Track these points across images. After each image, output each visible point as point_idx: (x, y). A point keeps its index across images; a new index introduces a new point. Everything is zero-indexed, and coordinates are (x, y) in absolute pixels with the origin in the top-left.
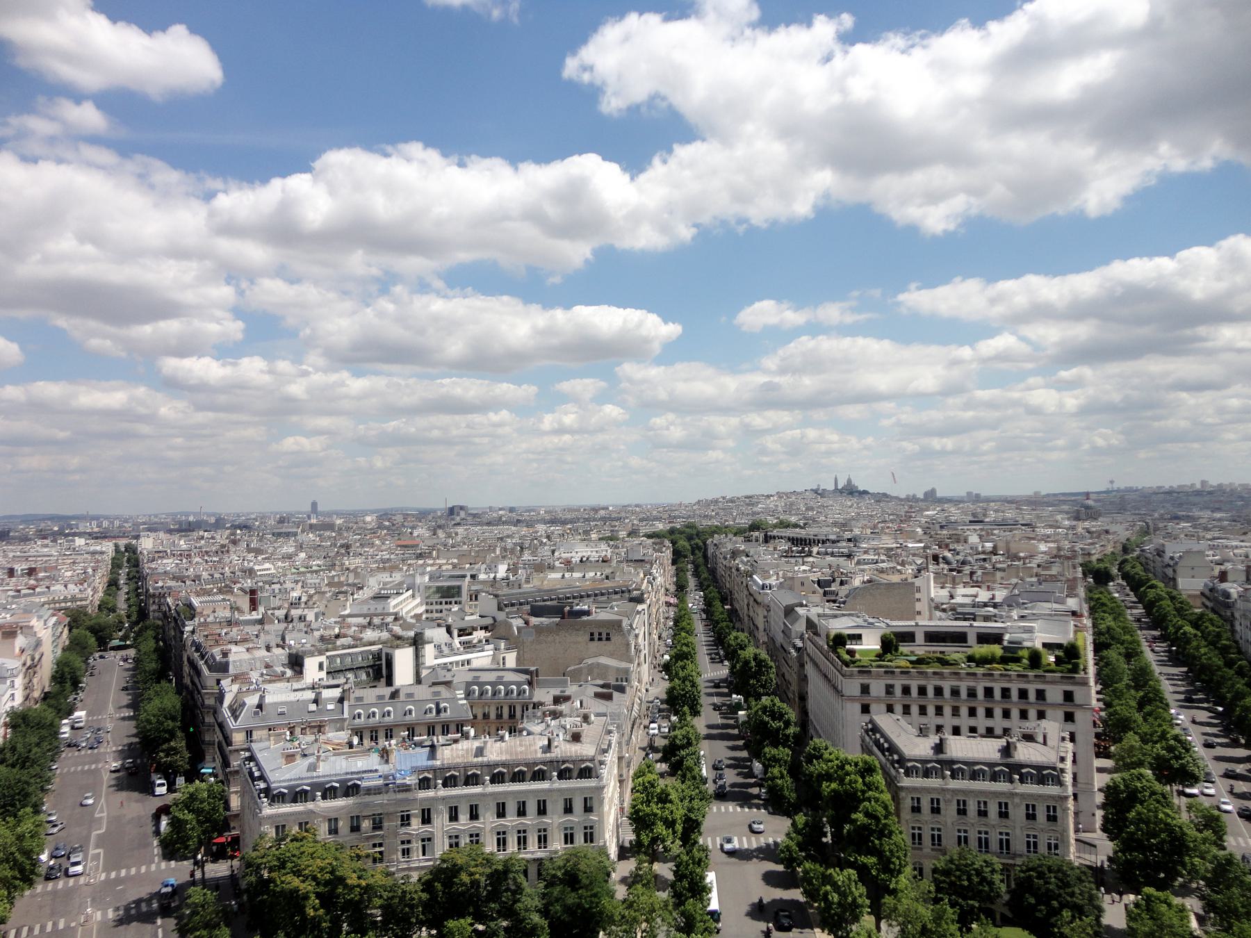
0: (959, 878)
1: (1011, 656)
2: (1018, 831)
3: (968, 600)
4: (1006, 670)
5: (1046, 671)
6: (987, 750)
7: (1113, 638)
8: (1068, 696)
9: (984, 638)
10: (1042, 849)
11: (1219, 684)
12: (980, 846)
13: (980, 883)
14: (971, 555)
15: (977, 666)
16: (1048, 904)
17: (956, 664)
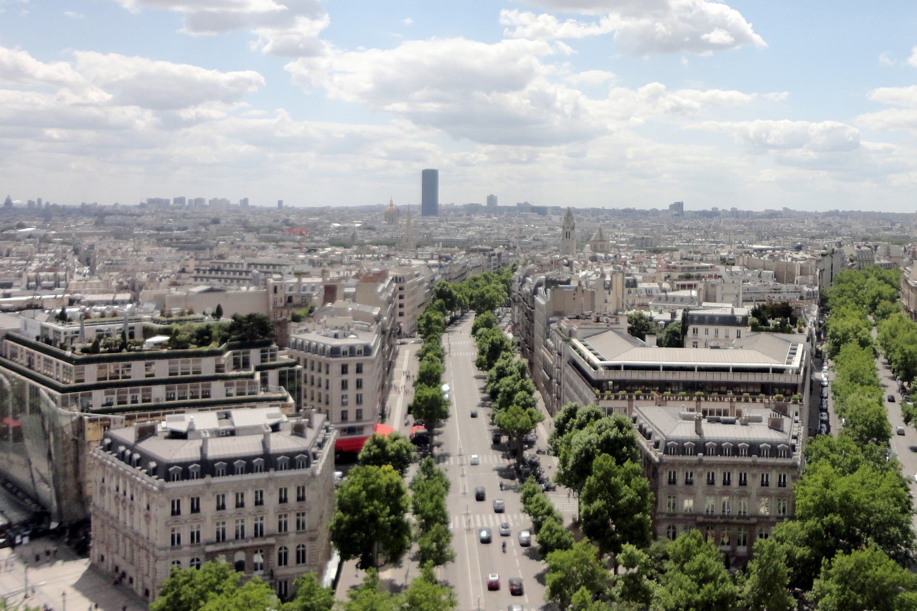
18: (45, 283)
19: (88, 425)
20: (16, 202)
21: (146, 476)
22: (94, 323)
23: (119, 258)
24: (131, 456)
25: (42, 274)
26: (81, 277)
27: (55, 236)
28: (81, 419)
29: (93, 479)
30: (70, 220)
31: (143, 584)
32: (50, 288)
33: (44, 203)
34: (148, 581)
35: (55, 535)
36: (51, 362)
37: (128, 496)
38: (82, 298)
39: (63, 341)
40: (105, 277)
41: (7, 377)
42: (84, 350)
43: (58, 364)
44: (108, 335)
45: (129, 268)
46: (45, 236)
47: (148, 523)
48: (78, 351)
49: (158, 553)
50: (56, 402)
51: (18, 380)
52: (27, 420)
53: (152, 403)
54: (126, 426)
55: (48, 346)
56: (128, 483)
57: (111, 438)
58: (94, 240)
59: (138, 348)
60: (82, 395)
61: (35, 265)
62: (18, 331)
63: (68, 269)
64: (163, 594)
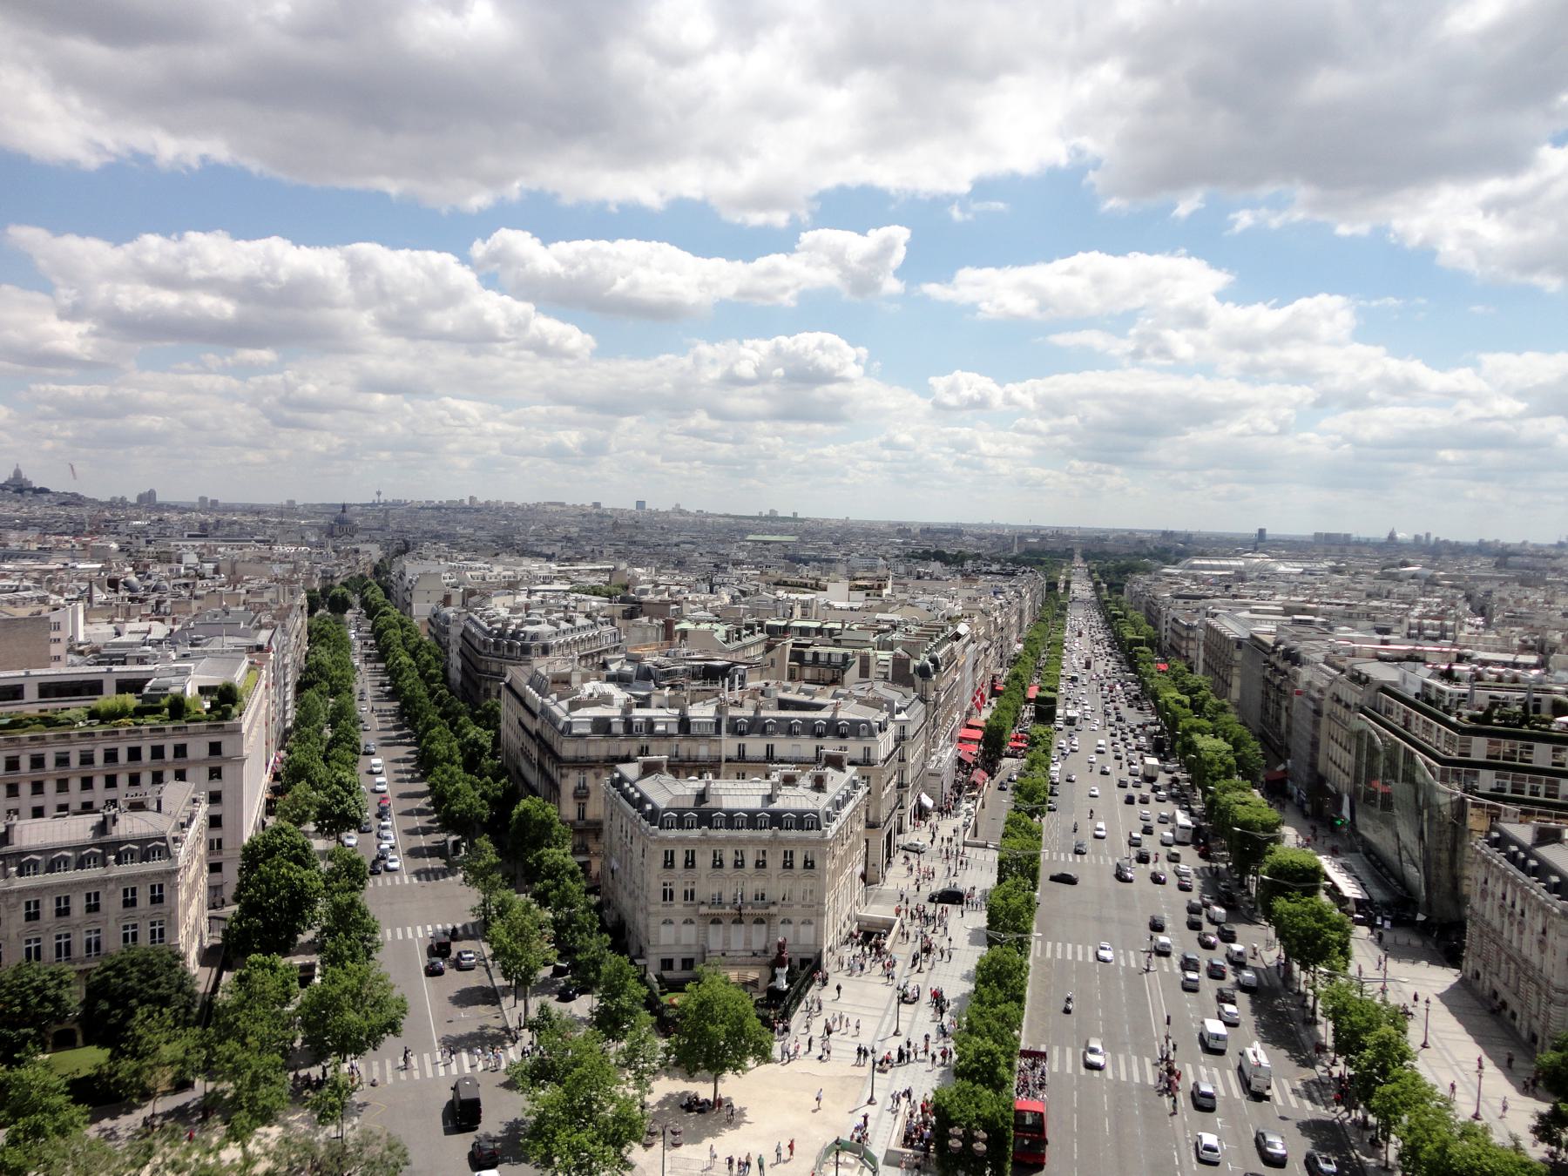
0: (10, 1004)
1: (149, 708)
2: (112, 923)
3: (137, 638)
4: (136, 724)
5: (187, 722)
6: (79, 829)
7: (321, 675)
8: (215, 749)
9: (124, 686)
10: (144, 940)
11: (417, 716)
12: (59, 954)
13: (40, 1004)
14: (167, 579)
15: (102, 723)
16: (124, 1005)
17: (71, 723)
18: (1428, 632)
19: (1471, 810)
20: (1400, 535)
21: (1544, 892)
22: (1488, 688)
23: (1524, 610)
24: (1525, 861)
25: (1426, 622)
26: (1473, 630)
27: (1443, 578)
28: (1462, 800)
29: (1473, 876)
30: (1463, 560)
31: (1530, 1025)
32: (1434, 639)
33: (1432, 538)
34: (1537, 1026)
35: (1423, 930)
36: (1431, 725)
37: (1518, 909)
38: (1473, 655)
39: (1447, 703)
40: (1505, 631)
41: (1379, 734)
42: (1472, 718)
43: (1439, 730)
44: (1505, 705)
45: (1537, 623)
46: (1432, 576)
47: (1542, 952)
48: (1464, 718)
49: (1552, 993)
50: (1433, 774)
51: (1392, 740)
52: (1398, 788)
53: (1559, 801)
54: (1521, 822)
55: (1429, 707)
56: (1519, 894)
57: (1500, 831)
58: (1494, 585)
59: (1543, 726)
60: (1466, 772)
61: (1418, 610)
62: (1394, 684)
63: (1457, 618)
64: (1557, 1049)
